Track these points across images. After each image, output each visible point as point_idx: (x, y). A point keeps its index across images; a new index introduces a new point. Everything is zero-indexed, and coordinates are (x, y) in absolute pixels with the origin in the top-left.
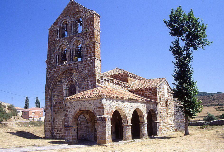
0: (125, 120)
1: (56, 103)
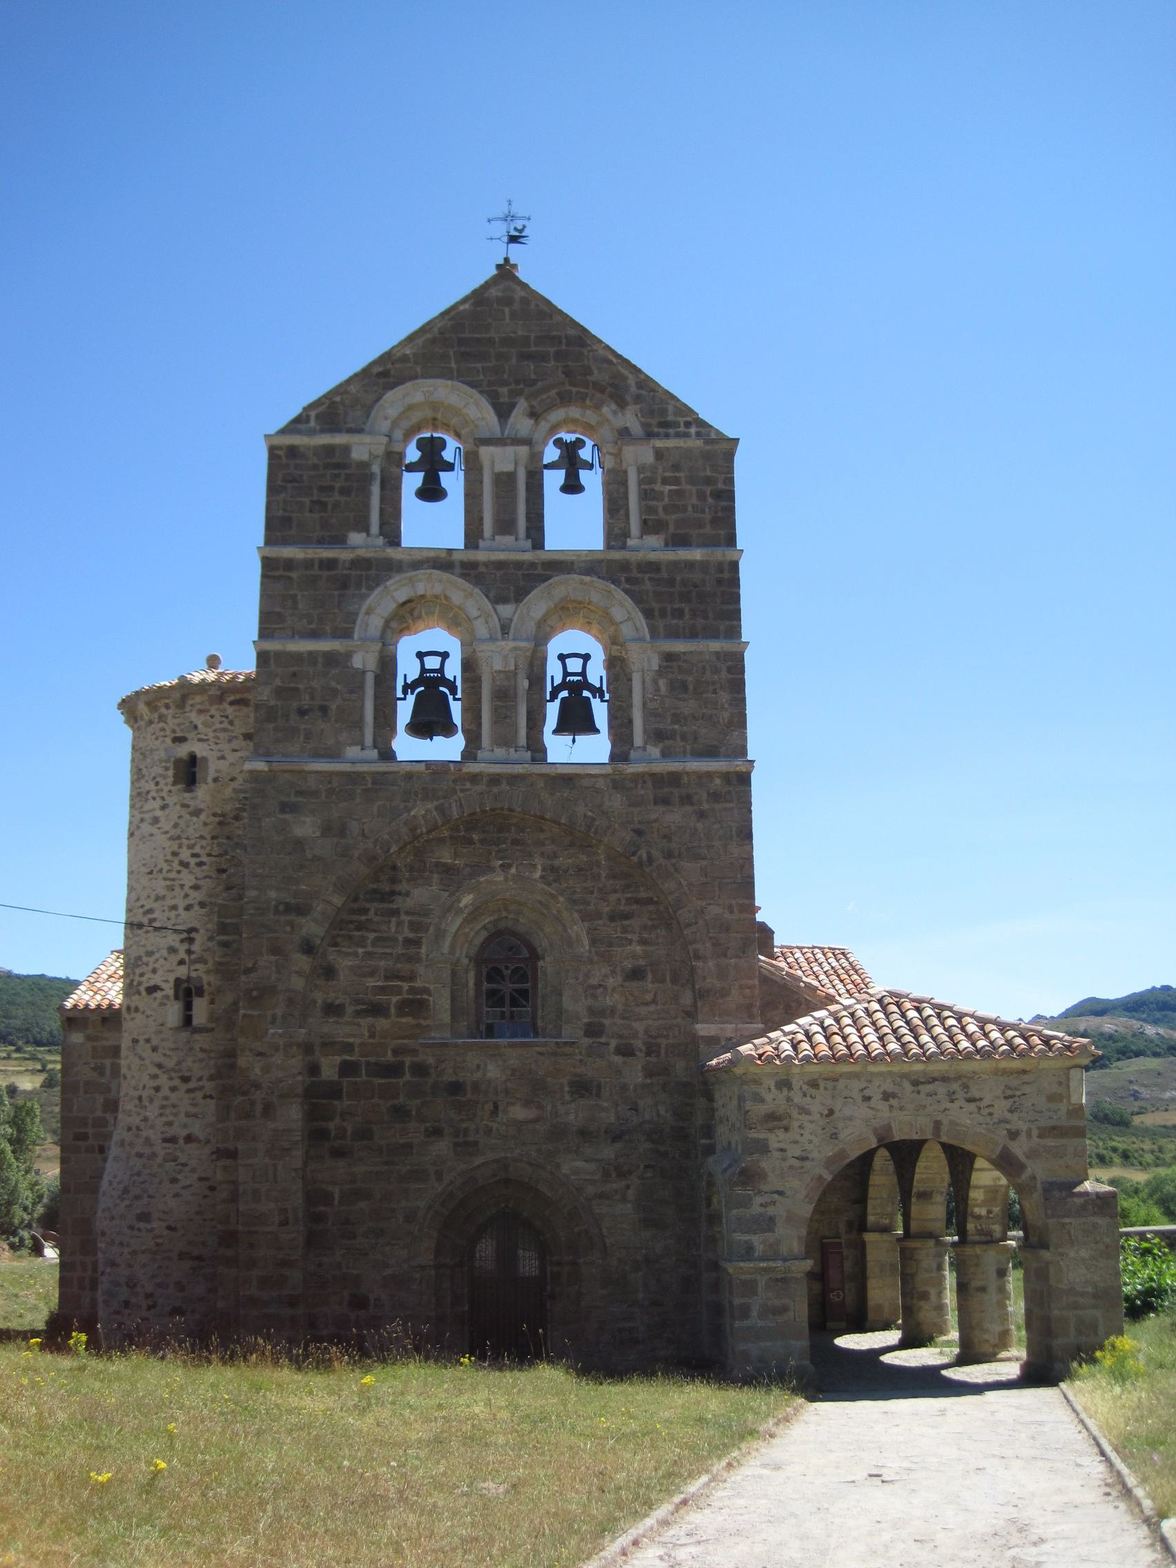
0: (989, 1212)
1: (348, 1069)
